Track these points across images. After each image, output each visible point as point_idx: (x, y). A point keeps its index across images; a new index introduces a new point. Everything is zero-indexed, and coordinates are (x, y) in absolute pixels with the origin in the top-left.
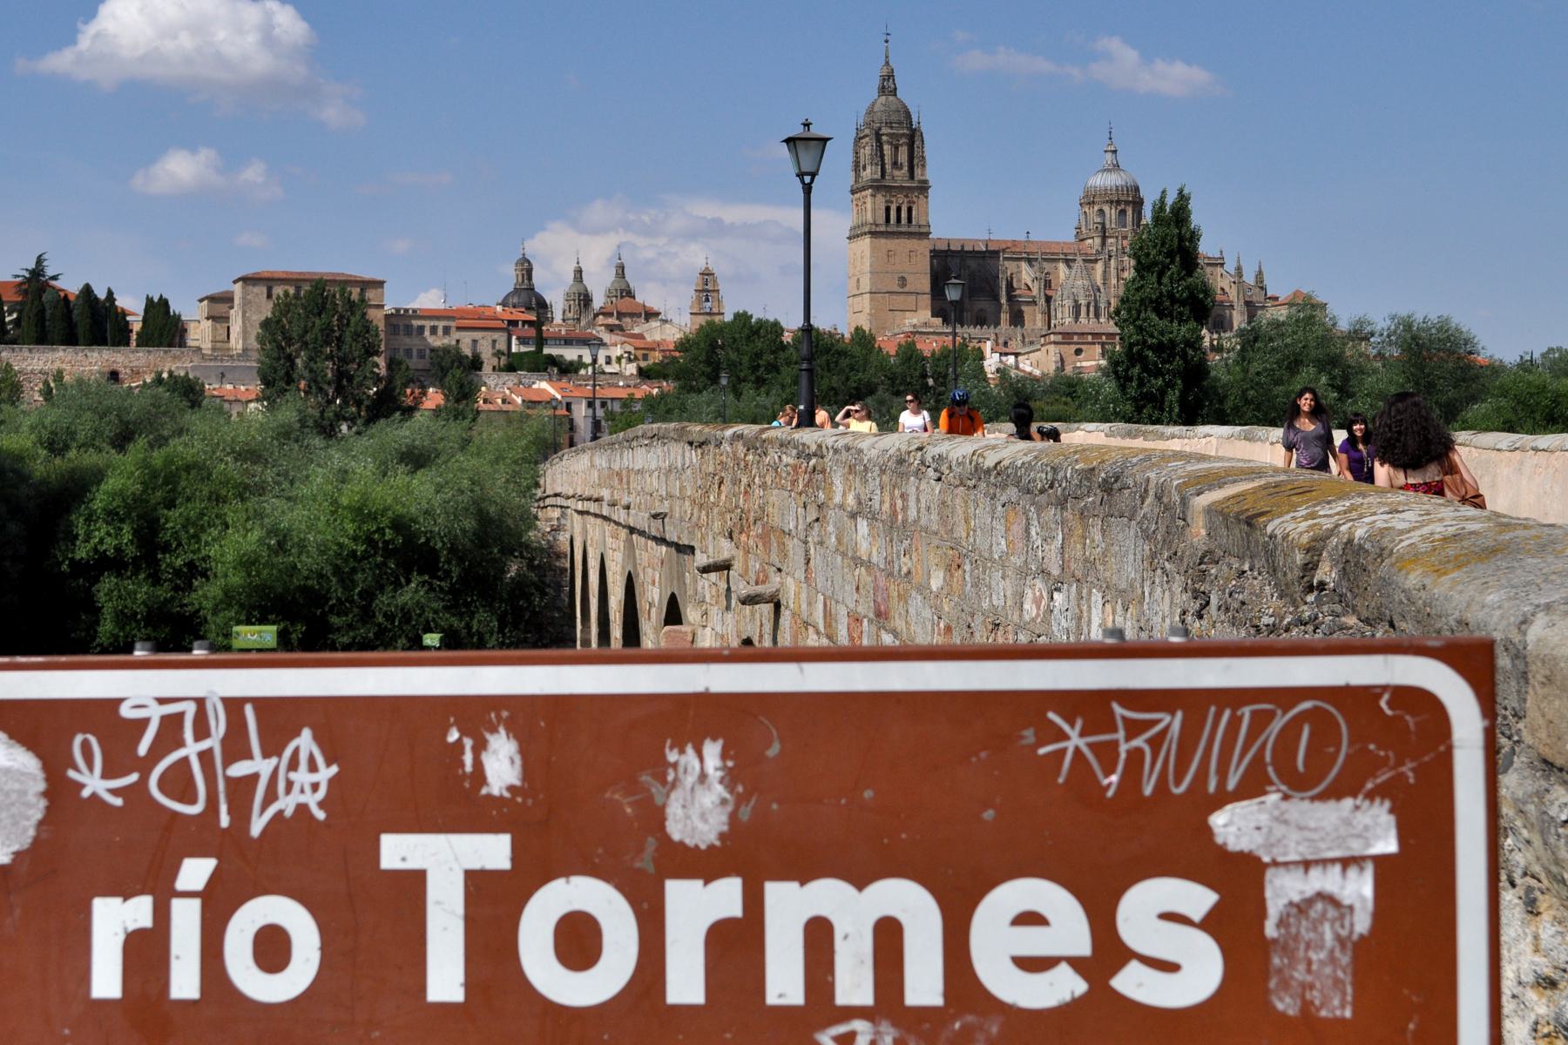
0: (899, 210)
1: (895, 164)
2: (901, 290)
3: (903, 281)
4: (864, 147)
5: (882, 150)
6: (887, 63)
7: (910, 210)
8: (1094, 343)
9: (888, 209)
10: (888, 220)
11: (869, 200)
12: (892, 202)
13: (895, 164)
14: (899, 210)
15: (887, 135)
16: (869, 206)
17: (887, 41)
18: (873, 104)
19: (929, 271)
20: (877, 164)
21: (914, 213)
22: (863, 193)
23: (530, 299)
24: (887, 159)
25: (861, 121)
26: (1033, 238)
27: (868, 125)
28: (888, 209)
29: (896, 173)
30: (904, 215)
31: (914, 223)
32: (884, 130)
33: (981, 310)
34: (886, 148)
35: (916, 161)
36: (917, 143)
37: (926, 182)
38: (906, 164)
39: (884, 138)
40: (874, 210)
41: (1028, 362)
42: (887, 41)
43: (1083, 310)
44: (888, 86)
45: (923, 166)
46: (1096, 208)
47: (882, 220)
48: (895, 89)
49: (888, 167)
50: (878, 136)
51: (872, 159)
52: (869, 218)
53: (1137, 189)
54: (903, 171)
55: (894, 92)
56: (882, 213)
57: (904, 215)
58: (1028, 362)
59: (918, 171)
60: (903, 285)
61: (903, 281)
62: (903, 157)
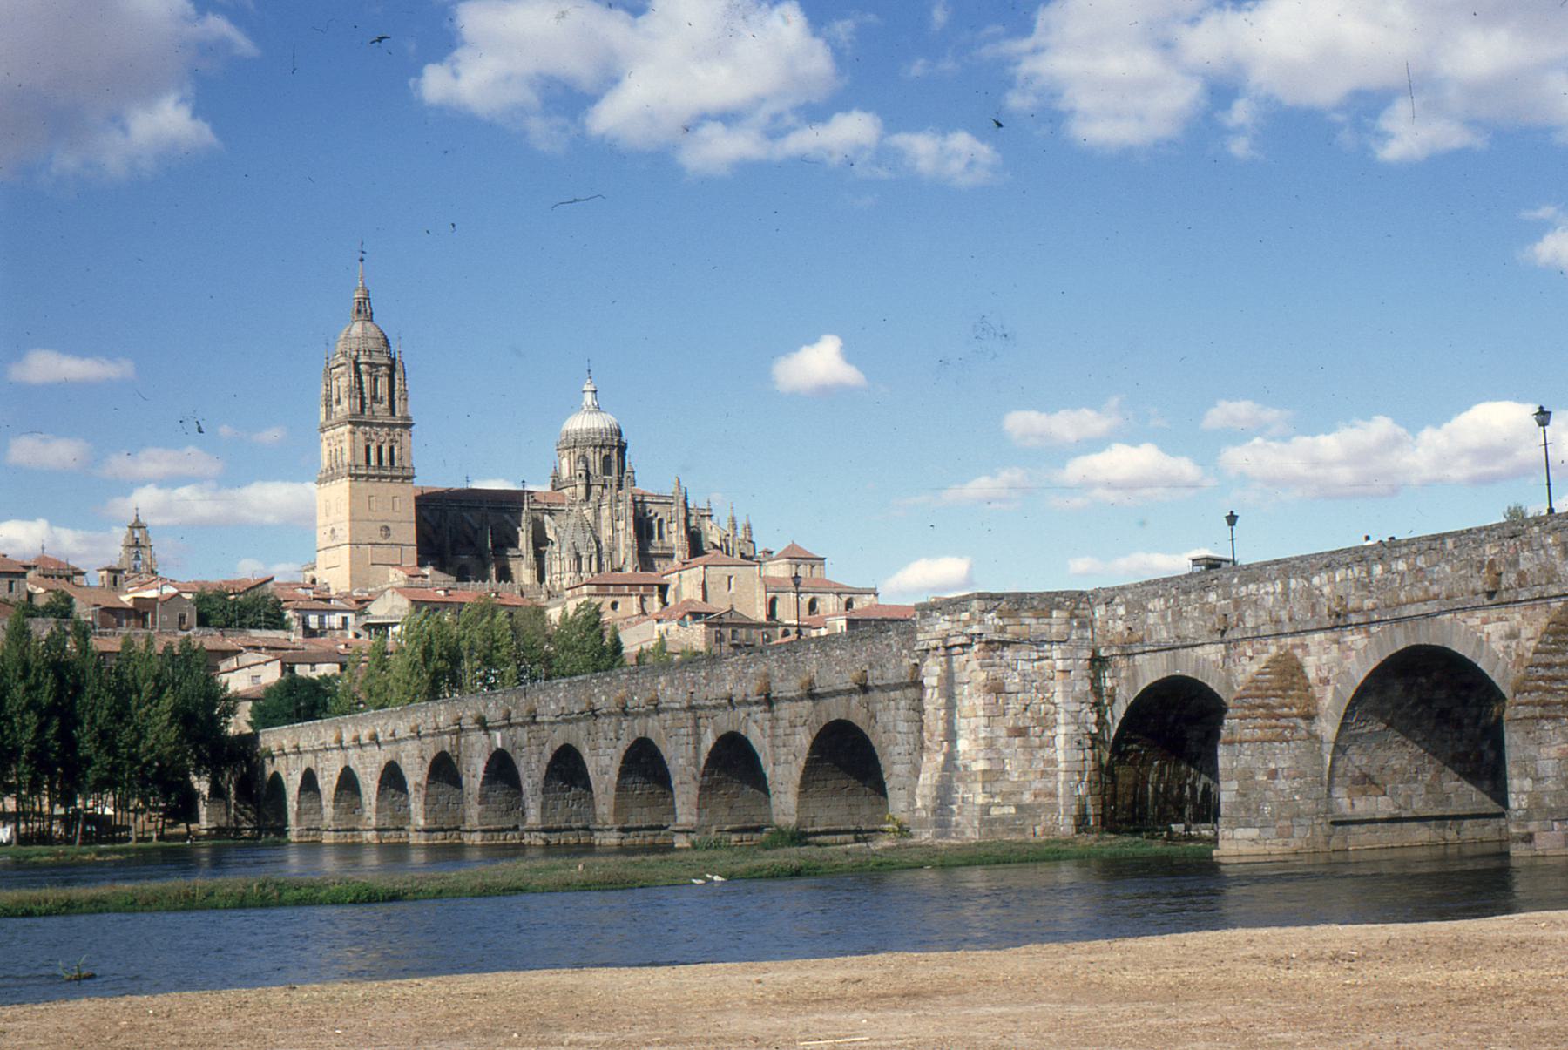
0: (380, 449)
1: (374, 397)
2: (384, 542)
4: (337, 379)
5: (361, 382)
8: (631, 595)
9: (368, 449)
11: (347, 437)
12: (373, 441)
13: (374, 397)
14: (380, 449)
15: (366, 363)
16: (346, 446)
17: (362, 260)
19: (414, 519)
20: (355, 397)
22: (342, 429)
24: (367, 395)
28: (368, 449)
29: (375, 406)
30: (385, 454)
31: (396, 465)
32: (362, 359)
34: (365, 378)
35: (397, 394)
38: (386, 398)
39: (362, 367)
40: (353, 451)
42: (362, 260)
43: (585, 563)
47: (362, 462)
48: (372, 314)
49: (368, 401)
50: (356, 365)
51: (350, 391)
52: (347, 457)
53: (620, 433)
54: (382, 406)
56: (363, 452)
57: (385, 454)
60: (388, 536)
62: (383, 387)
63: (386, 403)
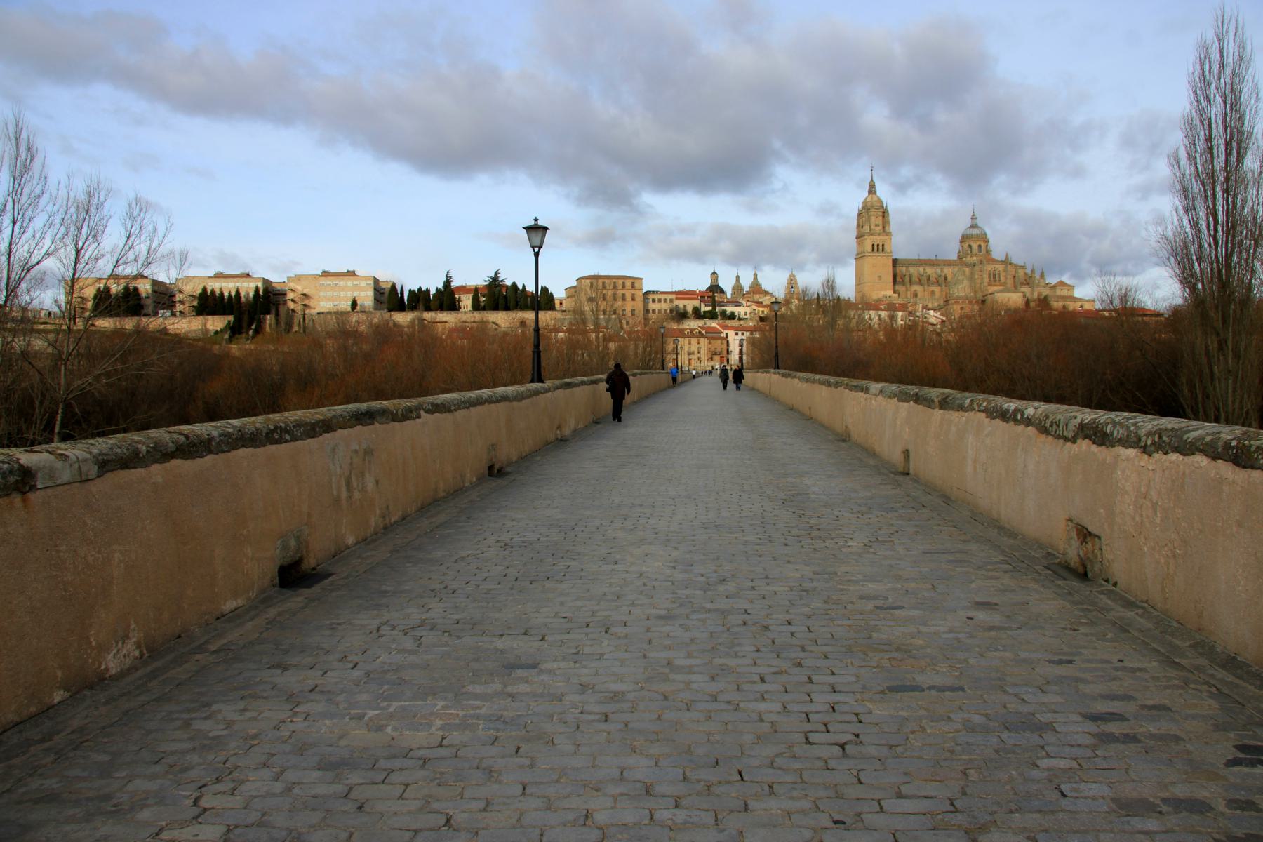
3: (880, 277)
6: (872, 180)
7: (883, 245)
9: (873, 245)
10: (873, 250)
18: (866, 198)
21: (885, 247)
23: (715, 288)
25: (861, 206)
26: (938, 258)
27: (863, 208)
28: (873, 245)
30: (881, 248)
33: (915, 291)
36: (886, 215)
37: (890, 233)
41: (939, 313)
44: (872, 190)
45: (889, 225)
46: (967, 245)
49: (872, 227)
55: (875, 193)
57: (881, 248)
58: (939, 313)
59: (887, 228)
61: (880, 277)
62: (880, 221)
63: (881, 227)
